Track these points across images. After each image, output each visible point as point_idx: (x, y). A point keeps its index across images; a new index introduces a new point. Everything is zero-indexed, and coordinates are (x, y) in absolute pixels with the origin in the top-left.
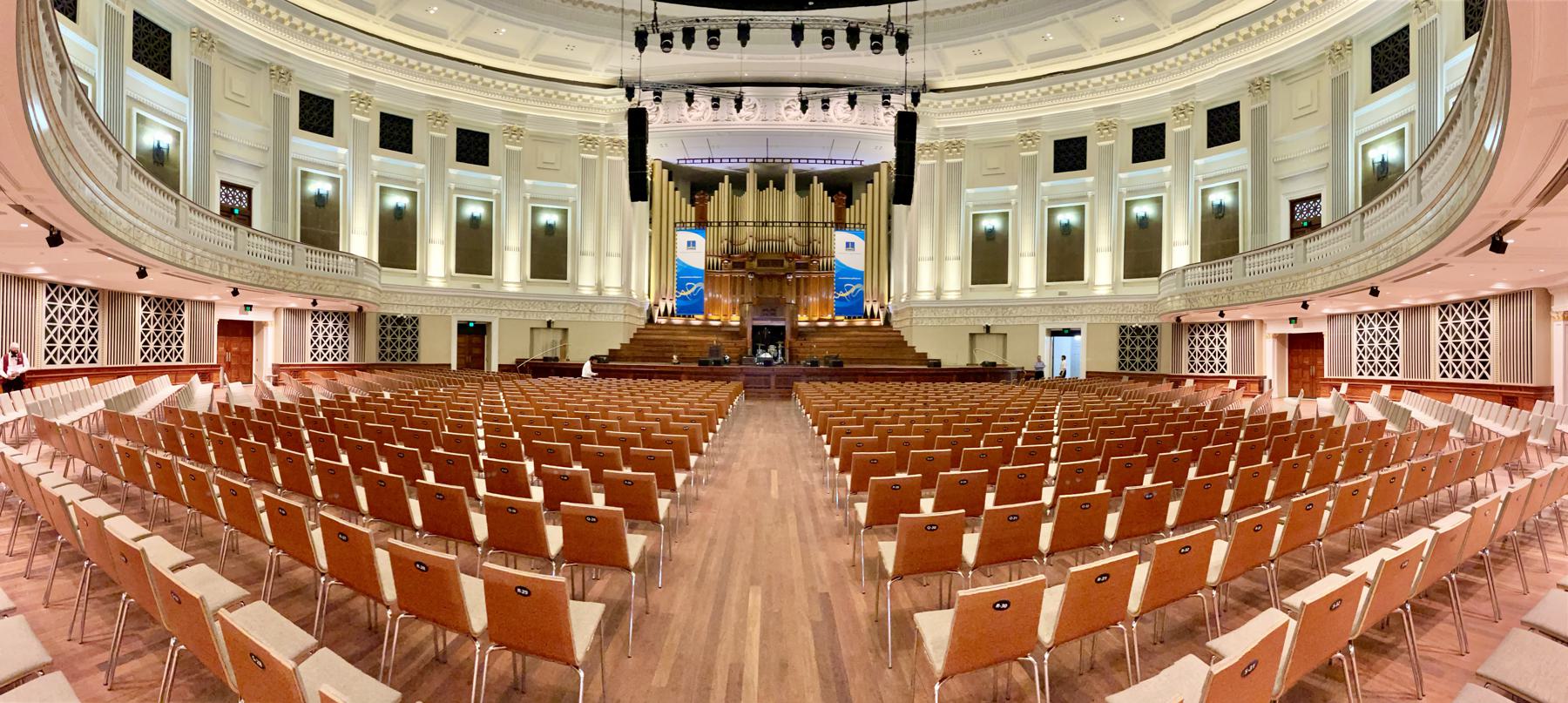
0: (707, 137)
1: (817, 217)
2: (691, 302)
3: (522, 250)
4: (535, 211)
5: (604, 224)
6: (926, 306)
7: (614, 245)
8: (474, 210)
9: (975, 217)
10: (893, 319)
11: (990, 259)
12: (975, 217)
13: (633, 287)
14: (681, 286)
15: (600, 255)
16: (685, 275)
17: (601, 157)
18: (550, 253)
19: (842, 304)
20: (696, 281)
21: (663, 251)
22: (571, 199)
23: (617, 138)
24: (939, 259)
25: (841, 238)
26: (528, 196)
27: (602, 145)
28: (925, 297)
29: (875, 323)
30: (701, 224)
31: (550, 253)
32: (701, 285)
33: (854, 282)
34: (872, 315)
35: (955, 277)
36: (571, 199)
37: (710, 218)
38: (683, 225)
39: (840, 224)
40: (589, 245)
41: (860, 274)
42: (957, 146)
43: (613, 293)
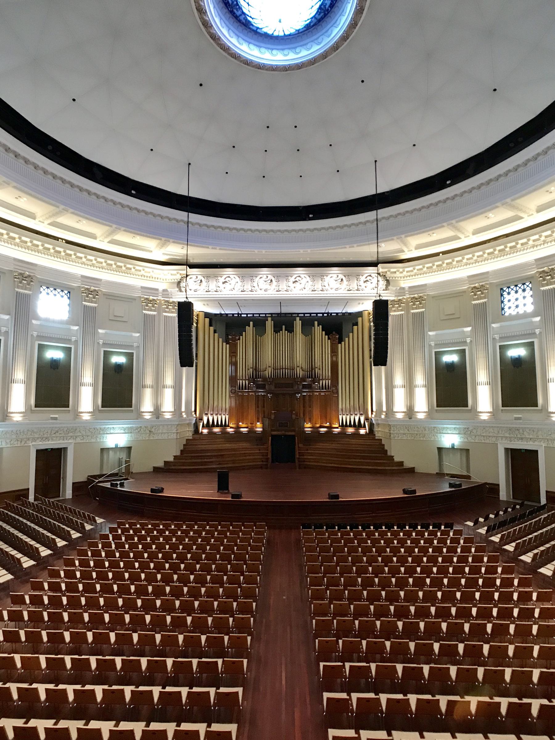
0: (237, 302)
3: (94, 385)
4: (107, 355)
5: (161, 364)
6: (400, 424)
7: (169, 380)
8: (54, 354)
9: (436, 353)
11: (451, 387)
12: (436, 353)
13: (183, 409)
15: (158, 388)
17: (159, 314)
18: (118, 389)
23: (171, 300)
24: (410, 387)
26: (101, 342)
27: (160, 304)
28: (400, 416)
29: (362, 432)
31: (118, 389)
35: (422, 402)
36: (135, 345)
40: (149, 380)
43: (168, 416)
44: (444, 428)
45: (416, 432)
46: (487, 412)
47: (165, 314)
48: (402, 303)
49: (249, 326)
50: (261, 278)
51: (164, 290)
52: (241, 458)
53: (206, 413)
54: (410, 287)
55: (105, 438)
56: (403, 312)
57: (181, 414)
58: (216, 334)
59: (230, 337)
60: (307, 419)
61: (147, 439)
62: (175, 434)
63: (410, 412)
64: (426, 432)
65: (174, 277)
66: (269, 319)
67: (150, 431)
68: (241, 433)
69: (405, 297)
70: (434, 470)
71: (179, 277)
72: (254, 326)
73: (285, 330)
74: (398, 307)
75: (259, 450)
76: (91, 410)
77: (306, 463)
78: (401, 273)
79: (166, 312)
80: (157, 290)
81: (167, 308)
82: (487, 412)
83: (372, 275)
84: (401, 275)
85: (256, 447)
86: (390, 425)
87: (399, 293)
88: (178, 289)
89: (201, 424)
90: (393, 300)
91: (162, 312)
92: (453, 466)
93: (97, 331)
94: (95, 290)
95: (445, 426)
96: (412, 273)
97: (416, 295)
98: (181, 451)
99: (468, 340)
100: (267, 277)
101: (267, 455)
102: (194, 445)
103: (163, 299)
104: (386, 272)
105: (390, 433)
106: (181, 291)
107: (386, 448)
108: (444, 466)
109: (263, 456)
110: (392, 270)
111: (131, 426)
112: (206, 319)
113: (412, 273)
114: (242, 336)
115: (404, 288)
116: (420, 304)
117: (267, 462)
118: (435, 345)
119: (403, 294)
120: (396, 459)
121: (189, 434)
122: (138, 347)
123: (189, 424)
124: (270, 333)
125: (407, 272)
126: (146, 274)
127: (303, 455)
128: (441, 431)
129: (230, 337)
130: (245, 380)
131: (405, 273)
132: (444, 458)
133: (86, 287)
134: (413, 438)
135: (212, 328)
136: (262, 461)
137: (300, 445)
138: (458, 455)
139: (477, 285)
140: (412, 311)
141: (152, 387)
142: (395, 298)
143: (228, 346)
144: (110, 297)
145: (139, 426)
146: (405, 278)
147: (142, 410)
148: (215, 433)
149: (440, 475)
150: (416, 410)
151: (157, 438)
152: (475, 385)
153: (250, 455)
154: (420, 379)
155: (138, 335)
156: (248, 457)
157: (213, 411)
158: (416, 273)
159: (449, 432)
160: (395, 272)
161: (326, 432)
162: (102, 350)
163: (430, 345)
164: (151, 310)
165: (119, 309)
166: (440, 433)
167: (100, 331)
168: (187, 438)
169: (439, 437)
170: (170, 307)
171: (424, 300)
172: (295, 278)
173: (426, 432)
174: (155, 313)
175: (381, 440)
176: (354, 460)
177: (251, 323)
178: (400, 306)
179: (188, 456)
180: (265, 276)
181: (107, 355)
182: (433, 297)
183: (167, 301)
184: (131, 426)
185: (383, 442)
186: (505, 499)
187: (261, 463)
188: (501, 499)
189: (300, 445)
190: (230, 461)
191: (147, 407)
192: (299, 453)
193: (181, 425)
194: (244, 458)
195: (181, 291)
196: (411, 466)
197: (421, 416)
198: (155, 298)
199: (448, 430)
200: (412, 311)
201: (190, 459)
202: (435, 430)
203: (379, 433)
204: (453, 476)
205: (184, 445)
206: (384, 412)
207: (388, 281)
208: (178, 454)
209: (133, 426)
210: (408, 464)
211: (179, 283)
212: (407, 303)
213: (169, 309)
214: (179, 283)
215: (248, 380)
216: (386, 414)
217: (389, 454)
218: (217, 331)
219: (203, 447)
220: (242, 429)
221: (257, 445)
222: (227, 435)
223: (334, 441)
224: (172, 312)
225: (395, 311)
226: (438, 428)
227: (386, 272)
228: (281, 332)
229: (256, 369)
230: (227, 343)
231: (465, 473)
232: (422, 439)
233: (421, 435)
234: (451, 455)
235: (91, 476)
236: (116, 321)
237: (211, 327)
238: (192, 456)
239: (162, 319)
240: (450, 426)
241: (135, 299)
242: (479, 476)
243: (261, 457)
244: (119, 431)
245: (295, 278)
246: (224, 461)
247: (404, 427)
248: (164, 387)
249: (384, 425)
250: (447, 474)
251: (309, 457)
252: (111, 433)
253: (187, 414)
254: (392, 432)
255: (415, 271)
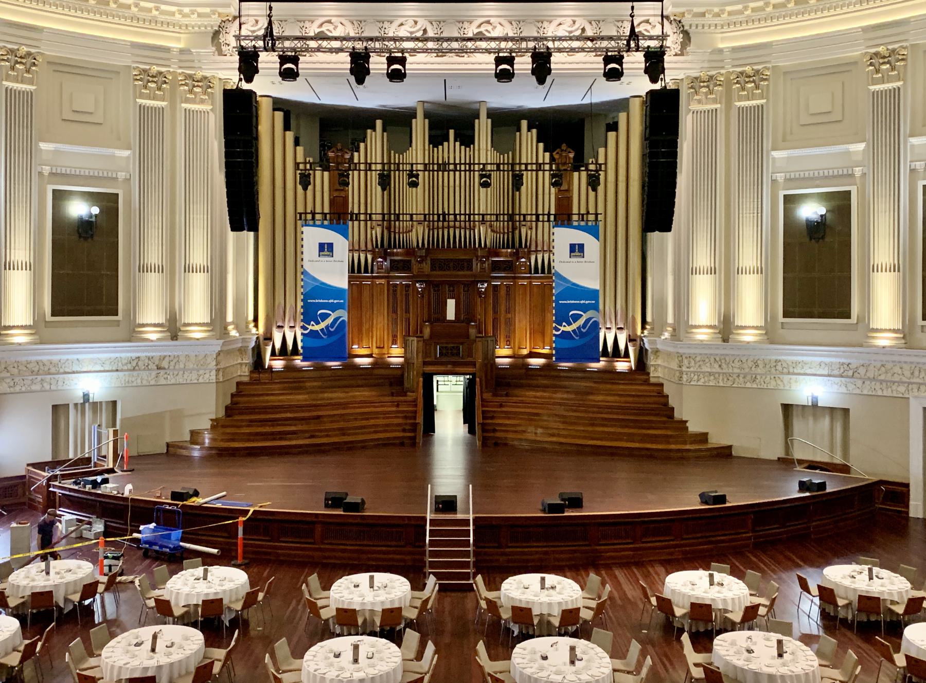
1: (526, 205)
2: (326, 340)
3: (34, 268)
5: (180, 218)
7: (199, 255)
9: (788, 199)
10: (652, 361)
12: (788, 199)
14: (309, 315)
15: (174, 271)
16: (315, 298)
19: (566, 344)
20: (334, 308)
21: (281, 265)
22: (122, 175)
23: (199, 74)
25: (564, 237)
26: (46, 170)
27: (175, 84)
28: (703, 335)
30: (339, 215)
32: (343, 314)
33: (585, 308)
34: (616, 353)
35: (752, 305)
36: (122, 175)
37: (354, 206)
38: (307, 217)
39: (563, 217)
40: (153, 256)
41: (593, 294)
42: (756, 78)
44: (797, 363)
45: (736, 371)
46: (890, 330)
47: (184, 105)
48: (716, 85)
49: (374, 128)
50: (402, 24)
51: (182, 51)
52: (358, 424)
53: (280, 324)
54: (735, 50)
55: (60, 383)
56: (718, 106)
57: (226, 328)
58: (300, 149)
59: (331, 154)
60: (502, 341)
61: (153, 383)
62: (214, 373)
63: (726, 327)
64: (759, 371)
65: (205, 21)
66: (420, 114)
67: (159, 368)
68: (357, 367)
69: (723, 71)
70: (774, 451)
71: (215, 21)
72: (384, 130)
73: (455, 141)
74: (706, 94)
75: (398, 406)
76: (30, 322)
77: (498, 434)
78: (718, 15)
79: (187, 101)
80: (167, 50)
81: (191, 92)
82: (890, 330)
83: (652, 20)
84: (717, 21)
85: (389, 399)
86: (680, 356)
87: (710, 61)
88: (214, 49)
89: (269, 349)
90: (696, 78)
91: (178, 100)
92: (813, 443)
93: (37, 145)
94: (29, 54)
95: (800, 358)
96: (740, 18)
97: (748, 69)
98: (227, 408)
99: (858, 171)
100: (416, 22)
101: (415, 418)
102: (254, 395)
103: (180, 71)
104: (683, 14)
105: (681, 373)
106: (221, 53)
107: (672, 402)
108: (796, 444)
109: (406, 418)
110: (696, 10)
111: (118, 355)
112: (277, 113)
113: (740, 18)
114: (358, 150)
115: (721, 51)
116: (757, 87)
117: (414, 431)
118: (787, 180)
119: (720, 64)
120: (694, 427)
121: (244, 372)
122: (127, 180)
123: (242, 351)
124: (420, 147)
125: (730, 14)
126: (142, 15)
127: (492, 418)
128: (790, 371)
129: (331, 154)
130: (366, 251)
131: (725, 16)
132: (798, 425)
133: (10, 46)
134: (729, 383)
135: (290, 135)
136: (404, 431)
137: (486, 396)
138: (826, 421)
139: (881, 49)
140: (738, 104)
141: (161, 270)
142: (703, 75)
143: (326, 174)
144: (61, 67)
145: (135, 355)
146: (726, 29)
147: (141, 320)
148: (299, 370)
149: (786, 463)
150: (738, 322)
151: (173, 381)
152: (869, 269)
153: (375, 415)
154: (749, 255)
155: (126, 153)
156: (372, 422)
157: (295, 320)
158: (748, 16)
159: (809, 371)
160: (703, 15)
161: (543, 368)
162: (50, 188)
163: (774, 181)
164: (155, 98)
165: (85, 96)
166: (789, 373)
167: (43, 146)
168: (238, 380)
169: (785, 382)
170: (197, 90)
171: (766, 80)
172: (479, 26)
173: (759, 371)
174: (164, 104)
175: (662, 385)
176: (601, 429)
177: (379, 123)
178: (711, 93)
179: (242, 421)
180: (411, 22)
181: (59, 196)
182: (785, 73)
183: (190, 77)
184: (118, 355)
185: (666, 390)
186: (921, 516)
187: (401, 434)
188: (912, 514)
189: (488, 396)
190: (334, 430)
191: (151, 312)
192: (483, 412)
193: (229, 352)
194: (364, 423)
195: (221, 53)
196: (725, 442)
197: (748, 337)
198: (163, 69)
199: (806, 367)
200: (738, 104)
201: (248, 426)
202: (779, 368)
203: (658, 370)
204: (813, 466)
205: (233, 396)
206: (670, 325)
207: (686, 34)
208: (222, 413)
209: (123, 355)
210: (717, 439)
211: (216, 34)
212: (728, 84)
213: (195, 94)
214: (216, 34)
215: (373, 251)
216: (674, 330)
217: (677, 415)
218: (301, 140)
219: (273, 400)
220: (358, 361)
221: (392, 394)
222: (327, 373)
223: (560, 387)
224: (202, 102)
225: (699, 102)
226: (785, 361)
227: (683, 14)
228: (446, 144)
229: (389, 228)
230: (325, 168)
231: (838, 459)
232: (749, 385)
233: (749, 377)
234: (811, 420)
235: (34, 465)
236: (80, 124)
237: (287, 133)
238: (251, 421)
239: (180, 117)
240: (815, 358)
241: (119, 73)
242: (869, 465)
243: (400, 421)
244: (90, 368)
245: (479, 26)
246: (321, 431)
247: (712, 360)
248: (188, 269)
249: (669, 354)
250: (800, 462)
251: (507, 422)
252: (74, 372)
253: (237, 328)
254: (684, 369)
255: (748, 12)
